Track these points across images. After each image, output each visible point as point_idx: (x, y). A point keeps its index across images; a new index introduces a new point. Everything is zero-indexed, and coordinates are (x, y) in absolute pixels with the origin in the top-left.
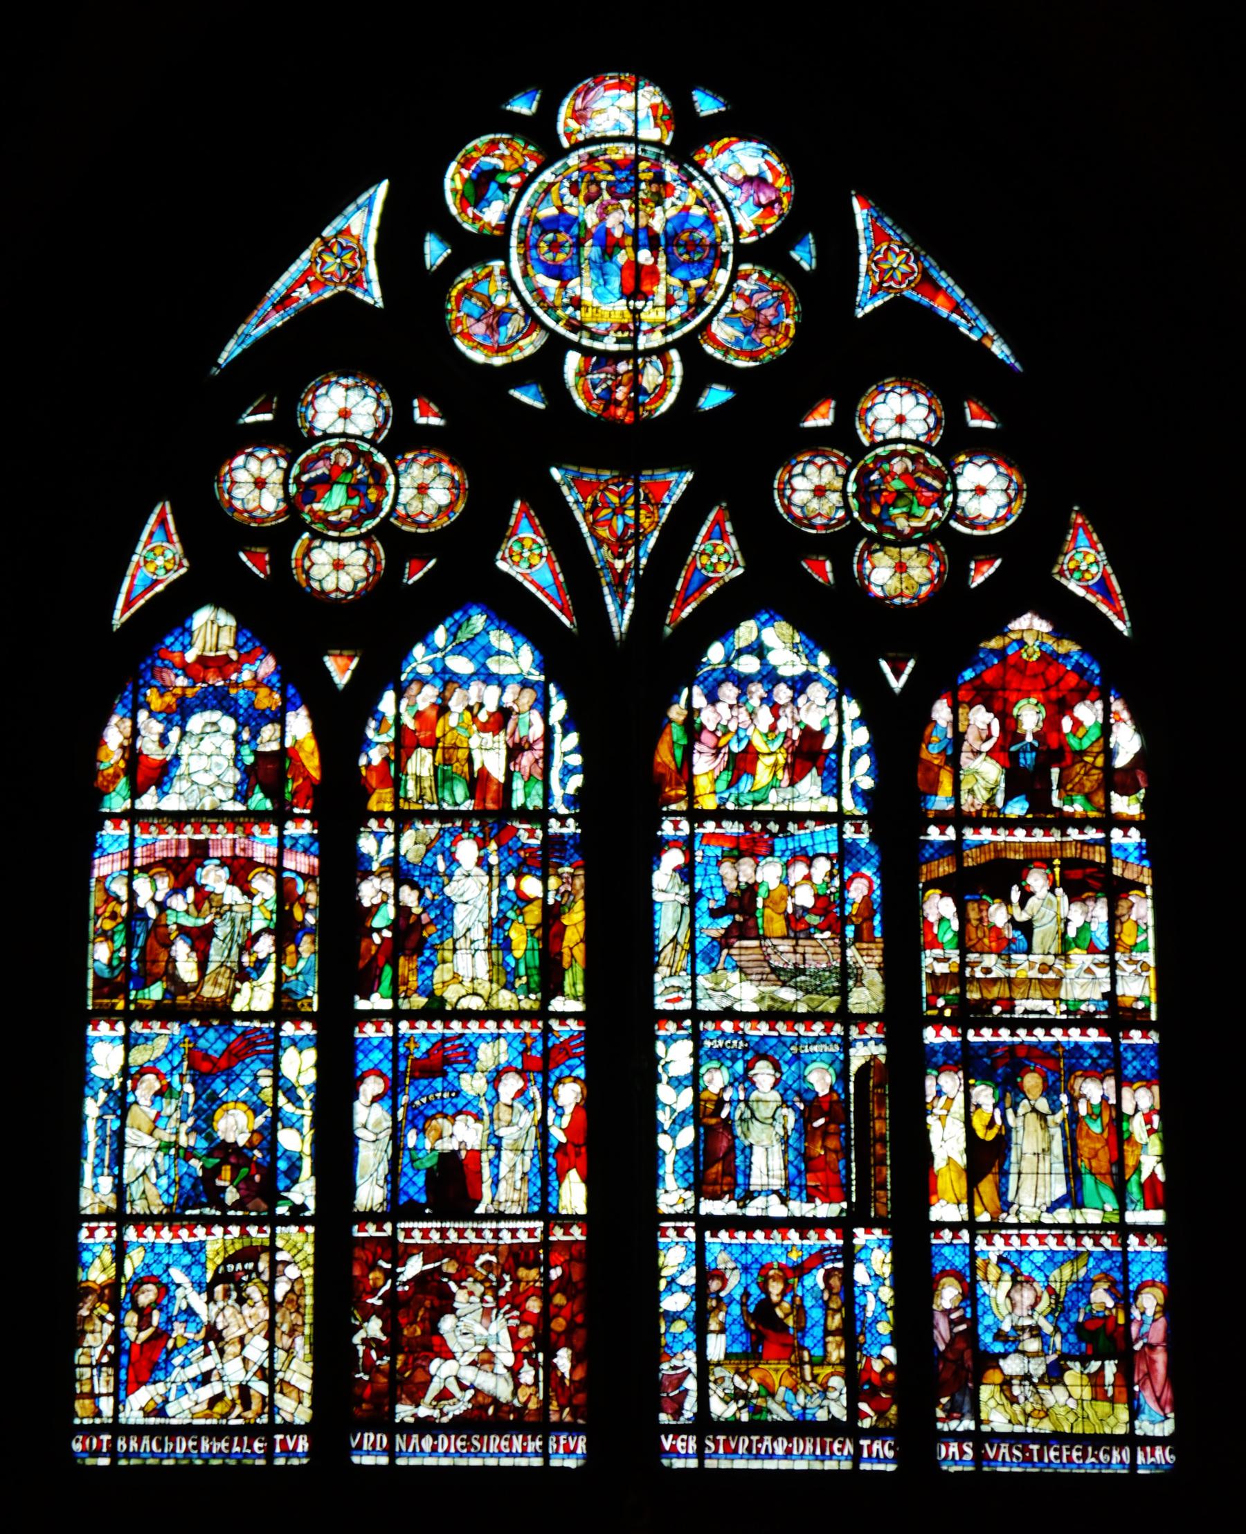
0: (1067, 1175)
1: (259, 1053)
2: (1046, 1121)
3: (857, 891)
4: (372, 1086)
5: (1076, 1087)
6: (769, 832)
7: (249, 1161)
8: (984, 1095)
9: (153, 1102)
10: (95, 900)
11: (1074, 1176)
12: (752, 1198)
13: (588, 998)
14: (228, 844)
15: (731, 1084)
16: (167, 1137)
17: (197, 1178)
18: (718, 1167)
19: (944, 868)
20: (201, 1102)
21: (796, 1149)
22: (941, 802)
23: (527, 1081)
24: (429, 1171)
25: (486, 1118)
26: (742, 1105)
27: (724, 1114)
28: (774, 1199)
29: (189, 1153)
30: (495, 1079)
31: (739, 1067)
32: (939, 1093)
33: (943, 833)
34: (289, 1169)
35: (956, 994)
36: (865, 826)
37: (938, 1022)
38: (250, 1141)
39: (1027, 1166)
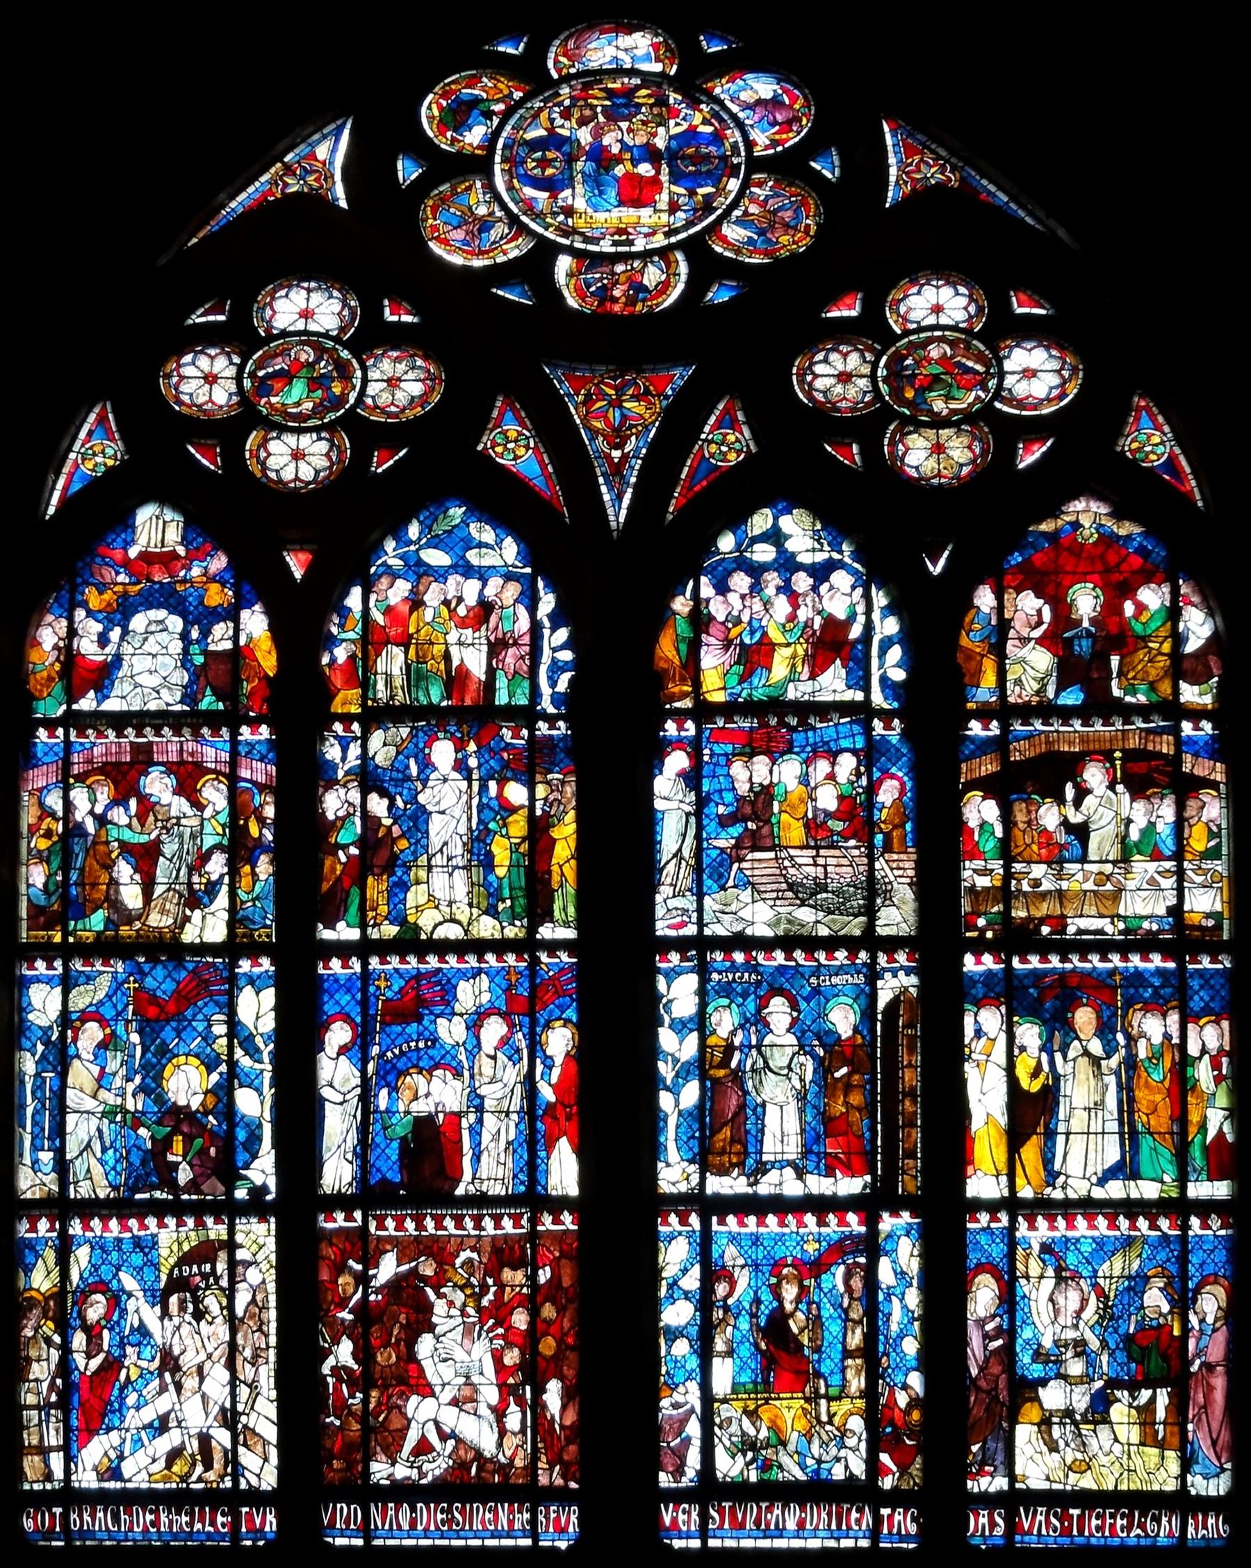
0: (1121, 1134)
1: (211, 994)
2: (1099, 1066)
3: (887, 794)
4: (339, 1034)
5: (1135, 1024)
6: (787, 726)
7: (202, 1129)
8: (1030, 1034)
9: (96, 1057)
10: (28, 816)
11: (1130, 1136)
12: (765, 1172)
13: (581, 923)
14: (174, 748)
15: (742, 1026)
16: (110, 1098)
17: (146, 1152)
18: (726, 1132)
19: (988, 766)
20: (149, 1055)
21: (814, 1107)
22: (985, 691)
23: (511, 1025)
24: (403, 1140)
25: (466, 1074)
26: (754, 1052)
27: (734, 1064)
28: (789, 1172)
29: (137, 1121)
30: (476, 1023)
31: (751, 1005)
32: (979, 1033)
33: (986, 728)
34: (248, 1139)
35: (999, 912)
36: (896, 722)
37: (979, 947)
38: (202, 1104)
39: (1077, 1124)
